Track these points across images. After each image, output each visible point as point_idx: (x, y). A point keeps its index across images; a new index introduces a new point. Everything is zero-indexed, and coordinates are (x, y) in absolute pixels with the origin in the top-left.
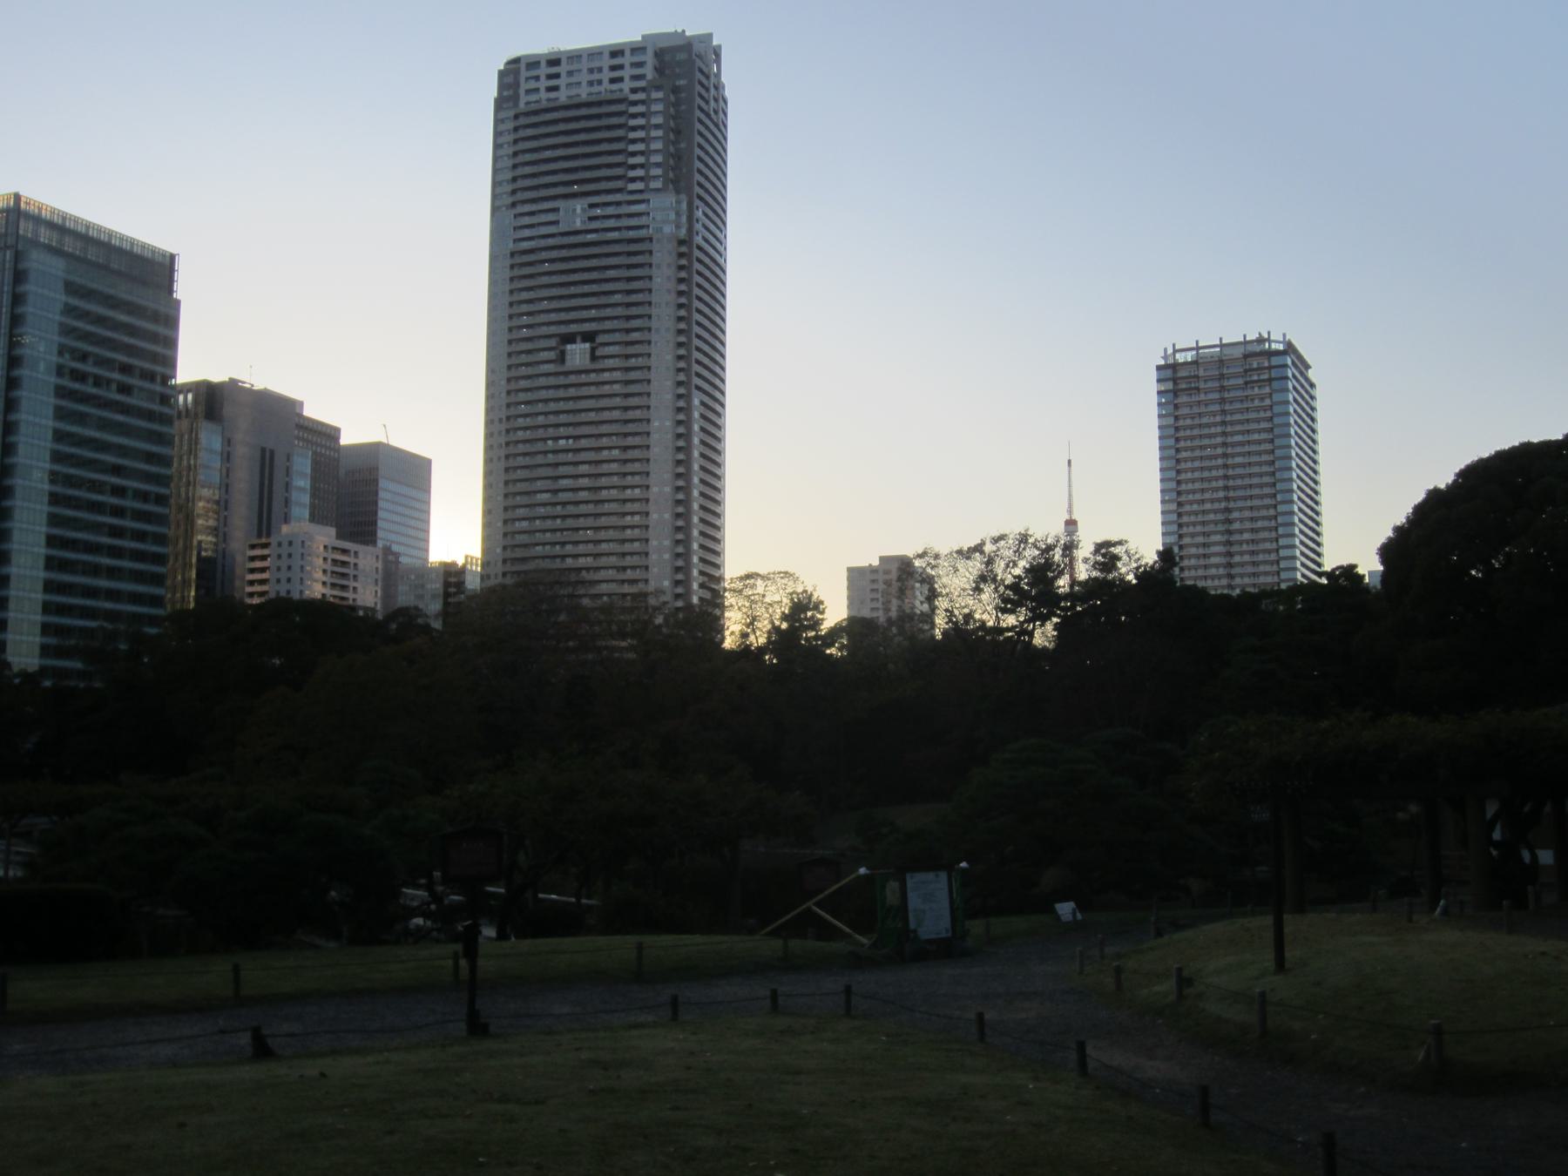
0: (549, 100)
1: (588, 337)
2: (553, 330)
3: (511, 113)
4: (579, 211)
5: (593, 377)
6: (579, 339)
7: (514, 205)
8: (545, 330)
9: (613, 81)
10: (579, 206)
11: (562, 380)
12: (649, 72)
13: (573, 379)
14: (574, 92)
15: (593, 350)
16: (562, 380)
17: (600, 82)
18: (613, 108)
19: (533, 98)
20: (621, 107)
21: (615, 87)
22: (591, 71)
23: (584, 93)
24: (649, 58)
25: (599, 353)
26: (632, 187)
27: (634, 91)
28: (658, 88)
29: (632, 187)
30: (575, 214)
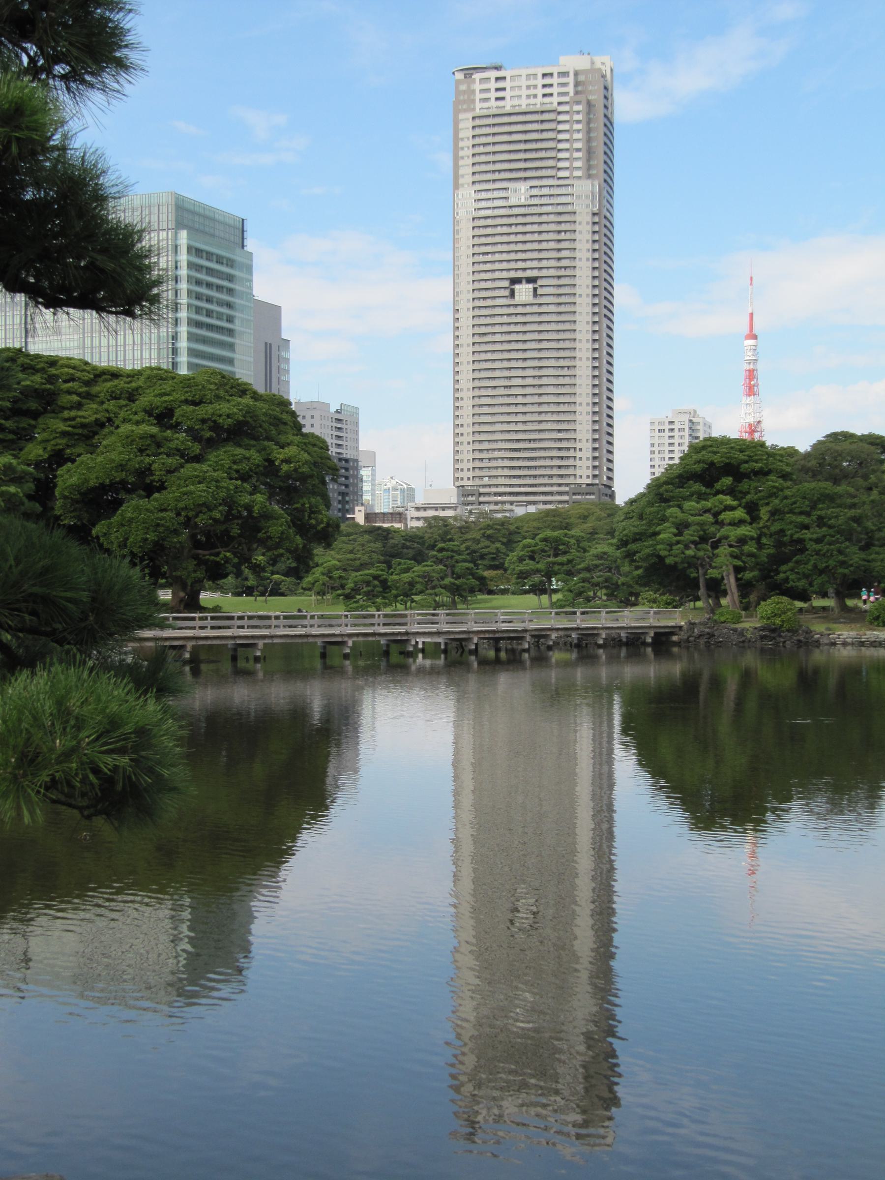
0: (497, 107)
1: (530, 280)
2: (505, 274)
3: (470, 115)
4: (523, 191)
5: (535, 309)
6: (524, 281)
7: (473, 183)
8: (497, 275)
9: (544, 95)
10: (523, 186)
11: (512, 310)
12: (571, 89)
13: (520, 310)
14: (516, 102)
15: (535, 290)
16: (512, 310)
17: (535, 96)
18: (546, 117)
19: (486, 105)
20: (552, 116)
21: (547, 100)
22: (528, 87)
23: (524, 104)
24: (571, 80)
25: (540, 291)
26: (561, 174)
27: (559, 104)
28: (578, 103)
29: (561, 174)
30: (520, 193)
